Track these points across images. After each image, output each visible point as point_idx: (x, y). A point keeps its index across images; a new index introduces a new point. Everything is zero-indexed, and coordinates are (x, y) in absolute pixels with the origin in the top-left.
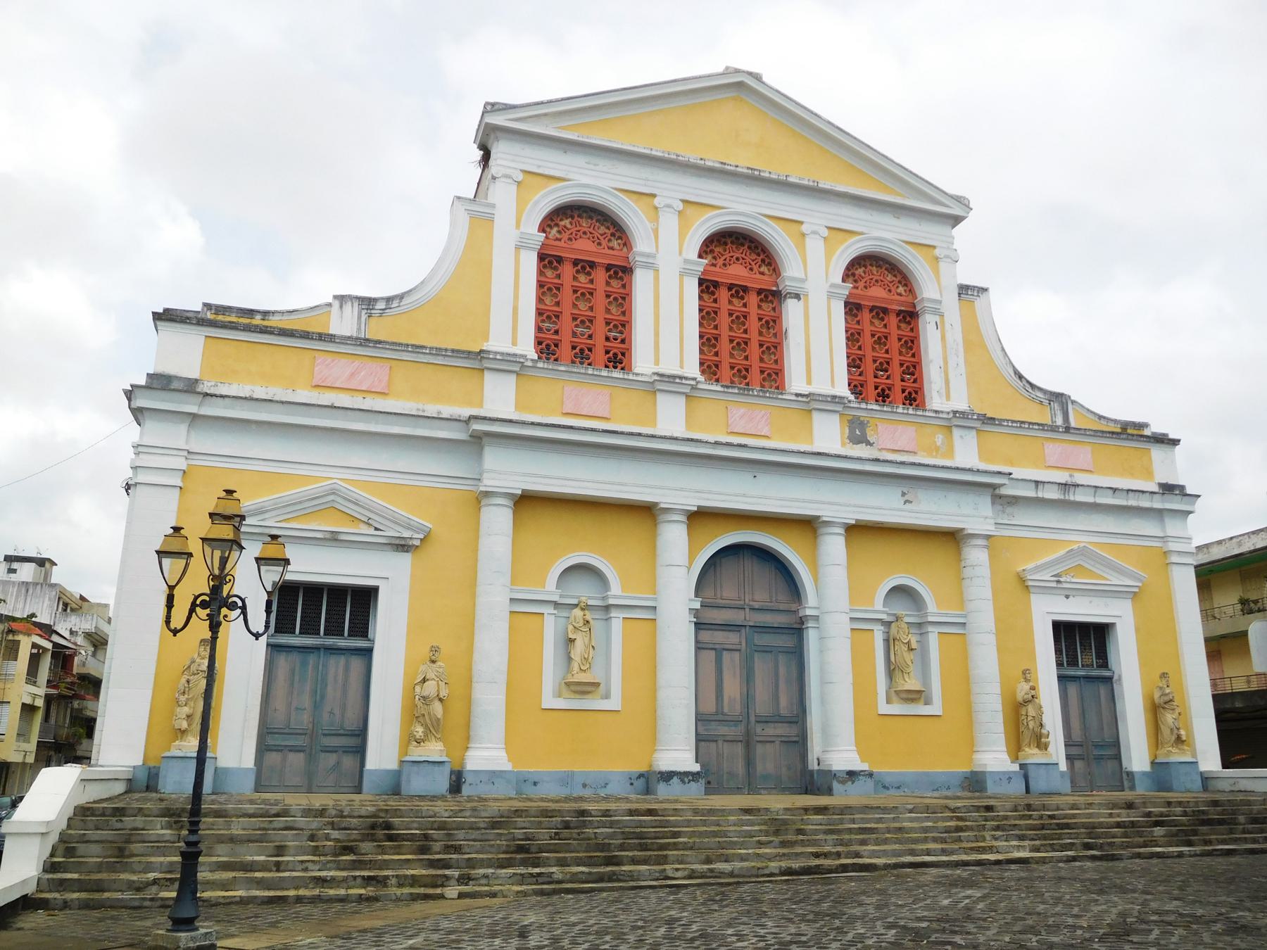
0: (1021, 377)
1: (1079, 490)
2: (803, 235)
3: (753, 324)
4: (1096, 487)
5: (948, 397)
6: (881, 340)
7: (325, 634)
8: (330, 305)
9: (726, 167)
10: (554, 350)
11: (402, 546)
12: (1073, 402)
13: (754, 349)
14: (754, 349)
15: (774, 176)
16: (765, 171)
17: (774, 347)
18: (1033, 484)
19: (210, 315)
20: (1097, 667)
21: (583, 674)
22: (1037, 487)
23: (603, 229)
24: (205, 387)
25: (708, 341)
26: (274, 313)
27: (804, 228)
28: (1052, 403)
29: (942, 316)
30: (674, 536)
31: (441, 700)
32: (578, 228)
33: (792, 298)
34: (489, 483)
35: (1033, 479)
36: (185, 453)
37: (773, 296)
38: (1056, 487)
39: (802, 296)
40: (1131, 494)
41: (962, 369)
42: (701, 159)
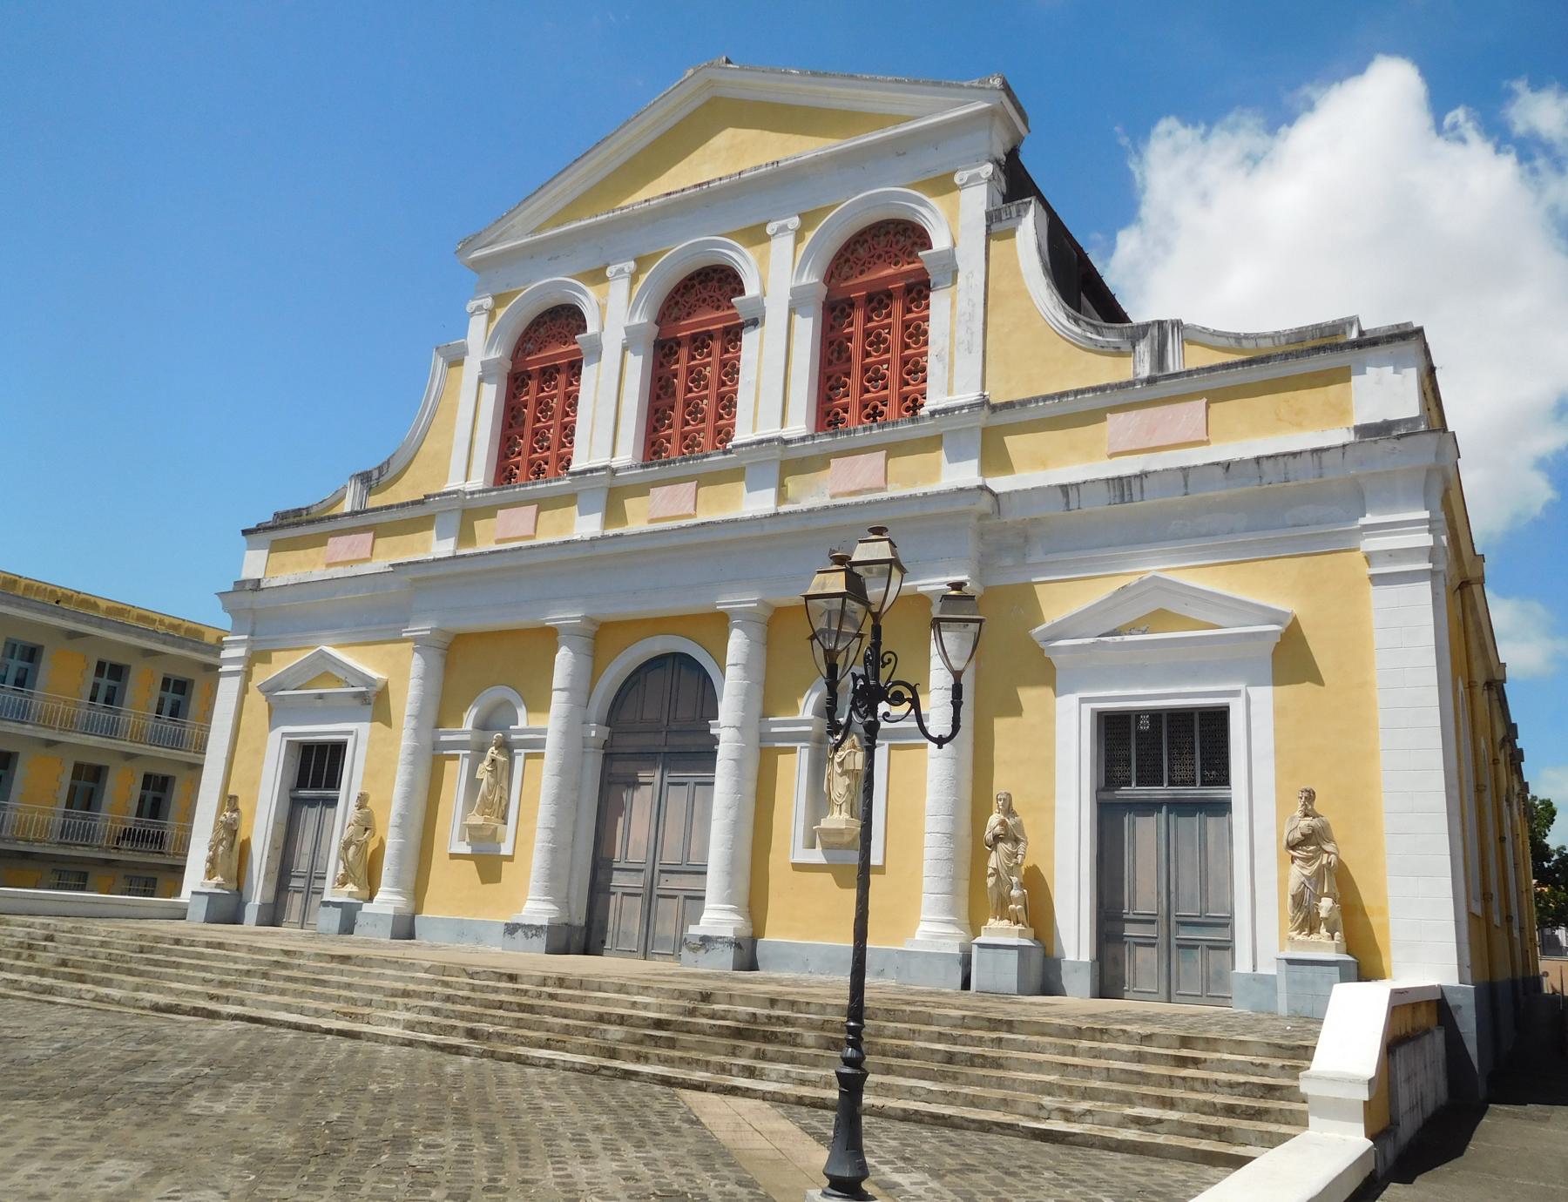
9: (672, 196)
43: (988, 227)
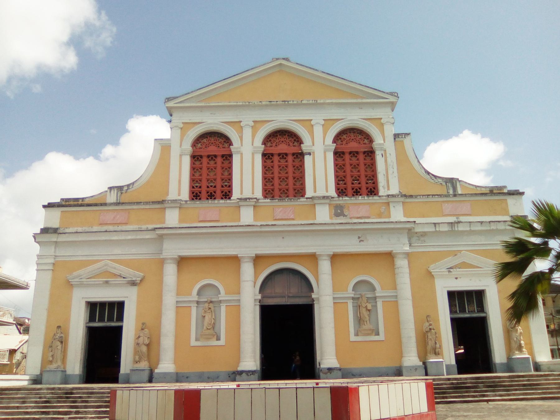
0: (428, 173)
1: (460, 225)
2: (312, 126)
3: (290, 169)
4: (470, 222)
5: (388, 189)
6: (355, 167)
7: (98, 321)
8: (106, 191)
9: (272, 103)
10: (199, 195)
11: (133, 283)
12: (460, 181)
13: (291, 181)
14: (291, 181)
15: (295, 102)
16: (290, 101)
17: (300, 178)
18: (433, 225)
19: (64, 203)
20: (477, 311)
21: (209, 331)
22: (435, 226)
23: (221, 140)
24: (61, 231)
25: (267, 180)
26: (86, 198)
27: (312, 123)
28: (447, 184)
29: (385, 151)
30: (247, 269)
31: (145, 345)
32: (210, 142)
33: (307, 155)
34: (165, 255)
35: (432, 222)
36: (54, 257)
37: (300, 156)
38: (446, 225)
39: (311, 153)
40: (492, 224)
41: (396, 174)
42: (260, 102)
43: (395, 139)
